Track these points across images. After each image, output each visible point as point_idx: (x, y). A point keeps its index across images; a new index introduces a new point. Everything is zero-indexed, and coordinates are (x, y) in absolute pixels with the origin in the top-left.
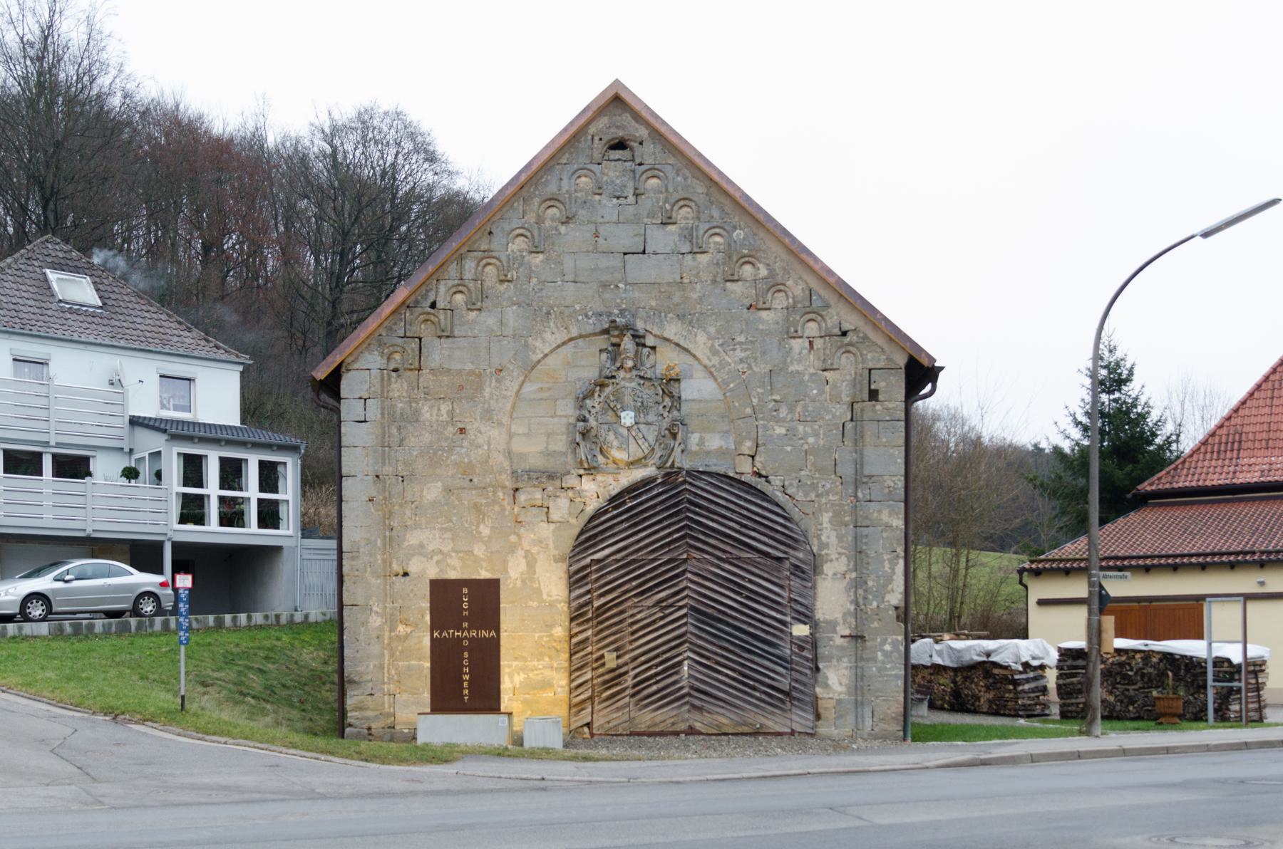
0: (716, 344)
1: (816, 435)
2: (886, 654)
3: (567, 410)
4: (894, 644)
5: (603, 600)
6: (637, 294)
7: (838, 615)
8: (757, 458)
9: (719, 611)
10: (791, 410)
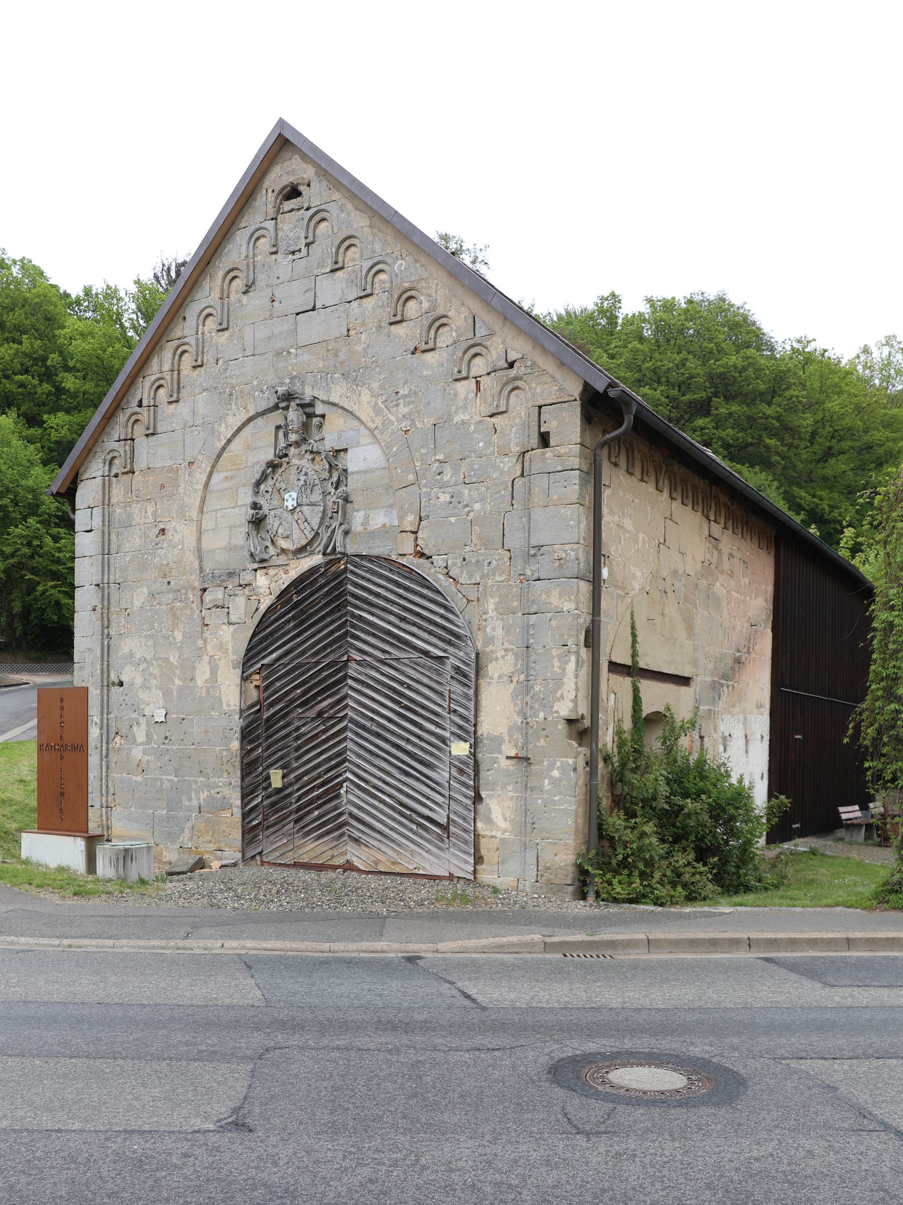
0: (379, 402)
1: (482, 500)
2: (555, 782)
3: (246, 497)
4: (562, 769)
5: (272, 711)
6: (306, 357)
7: (502, 730)
8: (420, 535)
9: (379, 725)
10: (455, 472)
